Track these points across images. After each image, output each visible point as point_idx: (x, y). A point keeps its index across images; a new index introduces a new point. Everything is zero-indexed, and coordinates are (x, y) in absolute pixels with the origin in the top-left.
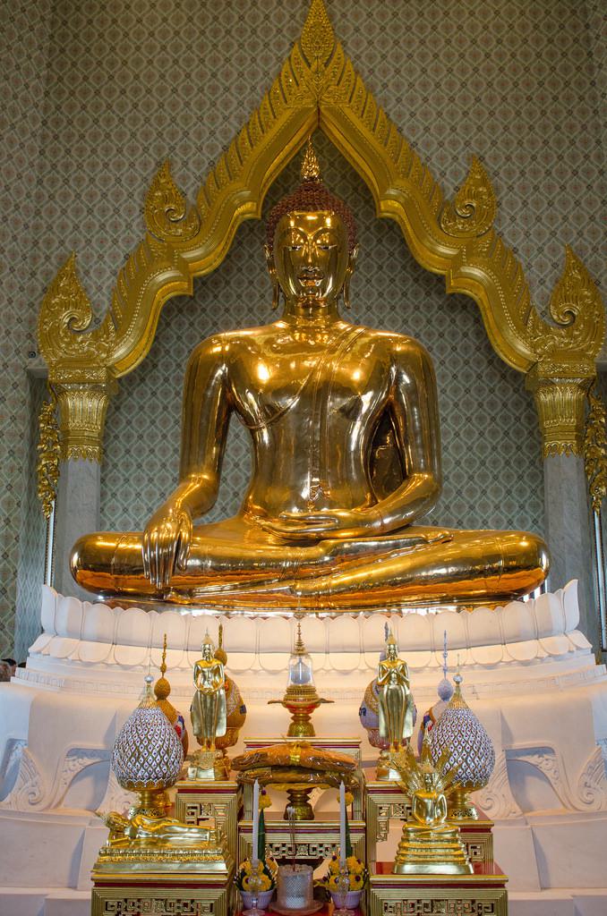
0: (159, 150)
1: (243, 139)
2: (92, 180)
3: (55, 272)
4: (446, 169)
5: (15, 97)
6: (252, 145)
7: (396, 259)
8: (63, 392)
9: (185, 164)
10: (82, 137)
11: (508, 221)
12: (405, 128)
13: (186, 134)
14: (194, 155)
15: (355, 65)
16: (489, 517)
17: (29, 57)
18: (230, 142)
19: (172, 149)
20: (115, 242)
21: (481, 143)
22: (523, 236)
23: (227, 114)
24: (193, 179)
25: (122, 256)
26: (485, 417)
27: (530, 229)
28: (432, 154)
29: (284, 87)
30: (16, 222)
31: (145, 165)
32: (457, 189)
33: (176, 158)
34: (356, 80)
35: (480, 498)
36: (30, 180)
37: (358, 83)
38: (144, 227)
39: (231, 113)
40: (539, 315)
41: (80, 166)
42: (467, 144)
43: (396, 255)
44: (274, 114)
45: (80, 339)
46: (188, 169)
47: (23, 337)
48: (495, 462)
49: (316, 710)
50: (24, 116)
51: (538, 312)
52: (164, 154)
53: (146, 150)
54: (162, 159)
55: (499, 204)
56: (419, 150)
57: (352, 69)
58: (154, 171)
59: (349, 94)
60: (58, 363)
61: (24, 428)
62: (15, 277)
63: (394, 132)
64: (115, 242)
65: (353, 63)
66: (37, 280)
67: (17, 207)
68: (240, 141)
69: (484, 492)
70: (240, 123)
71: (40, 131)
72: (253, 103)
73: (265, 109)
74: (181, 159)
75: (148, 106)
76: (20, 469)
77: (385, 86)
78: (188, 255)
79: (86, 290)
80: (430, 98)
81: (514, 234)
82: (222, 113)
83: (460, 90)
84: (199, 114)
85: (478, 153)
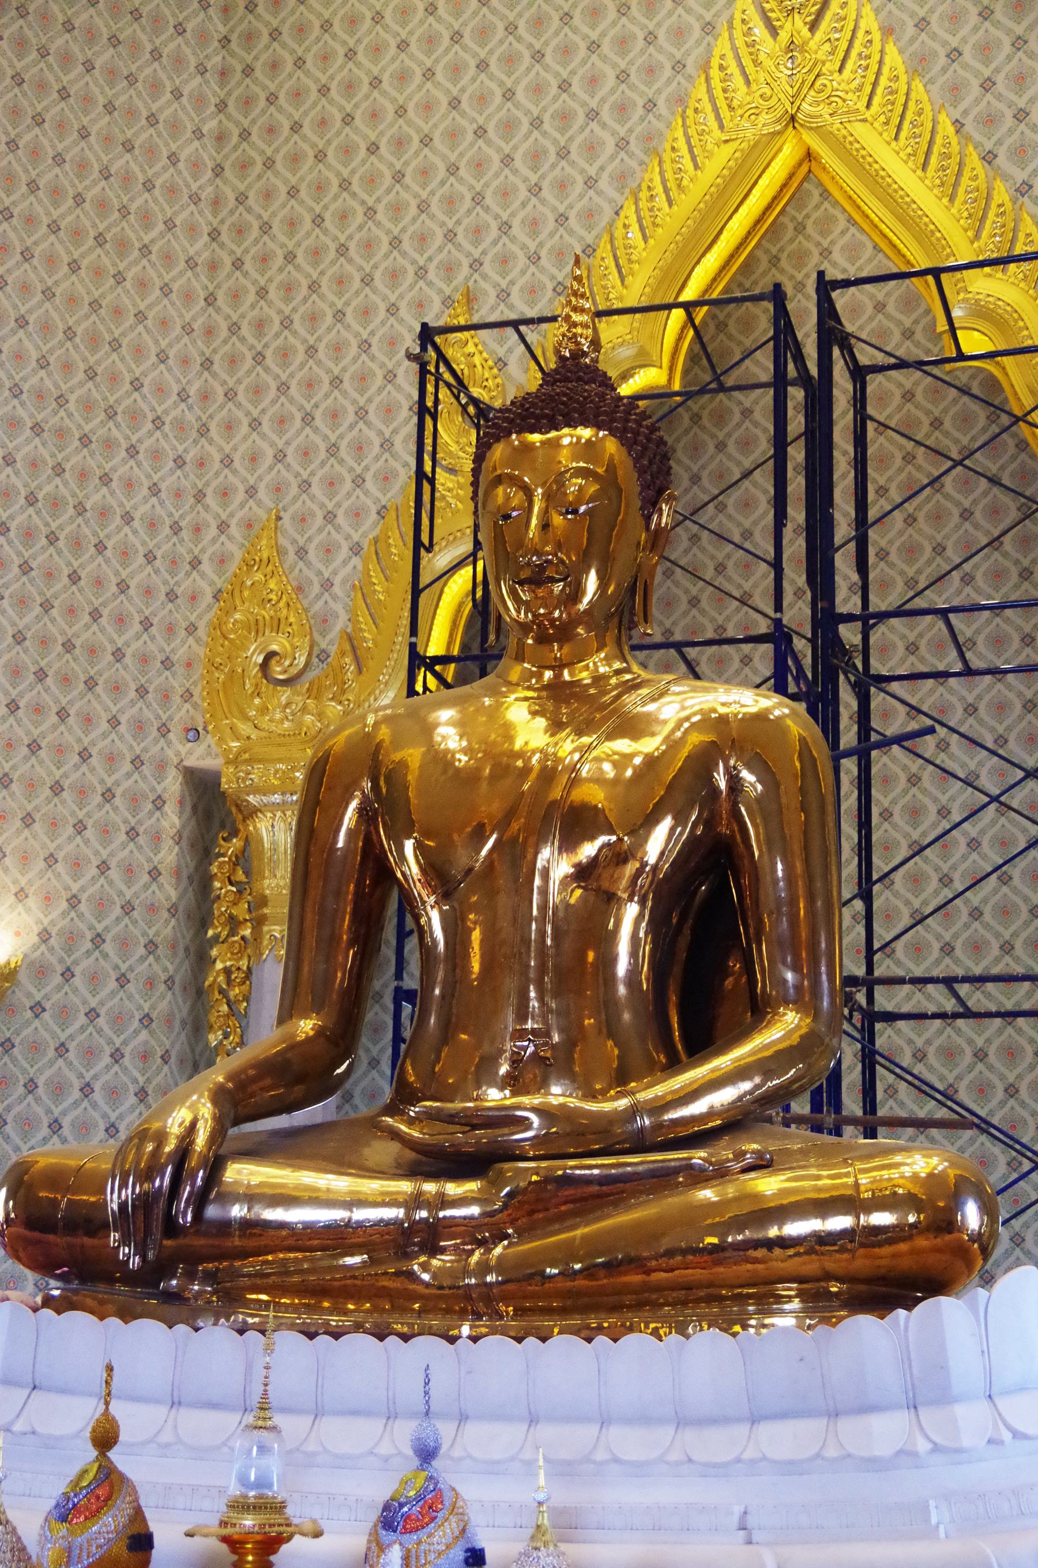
0: (449, 269)
1: (625, 226)
2: (311, 351)
3: (238, 555)
5: (148, 186)
6: (645, 238)
8: (251, 813)
10: (290, 257)
12: (1002, 152)
13: (505, 227)
14: (523, 272)
15: (884, 14)
17: (177, 94)
18: (598, 237)
19: (476, 265)
20: (359, 481)
23: (592, 171)
25: (374, 509)
29: (718, 93)
30: (156, 455)
33: (482, 284)
34: (882, 52)
36: (185, 361)
37: (887, 59)
41: (287, 323)
44: (694, 158)
45: (283, 700)
47: (177, 699)
49: (284, 1548)
50: (170, 225)
52: (460, 278)
53: (421, 272)
57: (874, 27)
59: (868, 89)
60: (243, 750)
61: (168, 891)
62: (157, 572)
63: (974, 160)
64: (359, 481)
65: (877, 11)
66: (203, 575)
67: (158, 422)
68: (619, 233)
70: (620, 190)
71: (206, 255)
72: (649, 139)
73: (673, 149)
74: (496, 285)
76: (170, 982)
79: (299, 589)
84: (534, 178)
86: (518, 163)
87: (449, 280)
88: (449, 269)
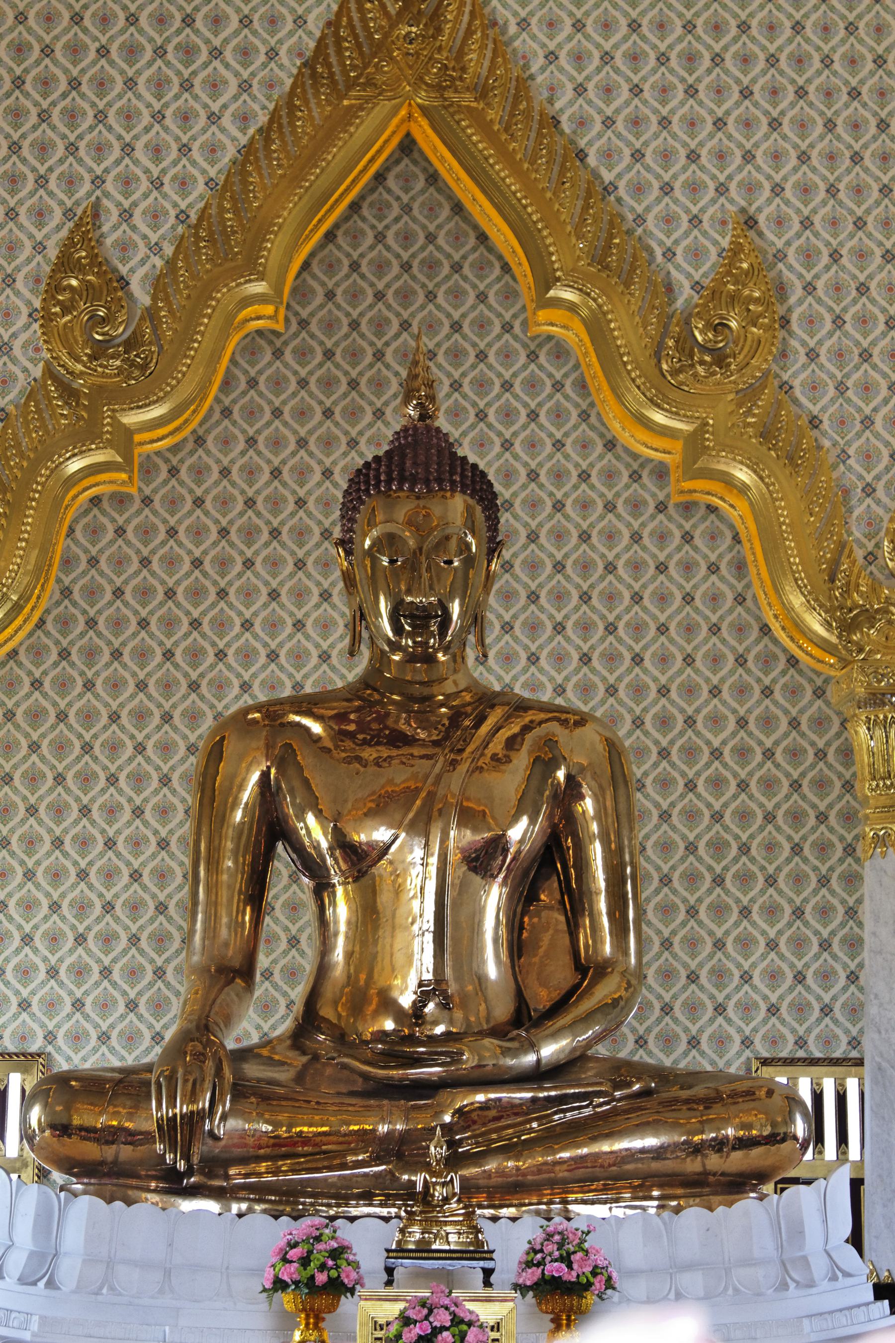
0: (70, 182)
4: (676, 242)
7: (567, 397)
9: (126, 215)
11: (803, 359)
13: (128, 149)
14: (146, 196)
16: (754, 965)
19: (98, 181)
21: (751, 188)
22: (831, 392)
23: (215, 107)
24: (142, 250)
26: (750, 750)
27: (847, 376)
28: (648, 209)
31: (40, 215)
32: (697, 286)
35: (737, 924)
38: (37, 350)
39: (225, 107)
40: (860, 561)
42: (722, 190)
43: (568, 389)
46: (134, 228)
48: (770, 847)
51: (859, 554)
52: (81, 193)
53: (42, 181)
54: (77, 203)
55: (785, 322)
56: (619, 200)
58: (58, 228)
69: (745, 912)
74: (119, 204)
75: (46, 83)
77: (552, 57)
78: (131, 419)
80: (646, 87)
81: (814, 387)
82: (206, 106)
83: (709, 71)
84: (157, 106)
85: (743, 210)
86: (141, 88)
87: (70, 193)
88: (70, 182)
